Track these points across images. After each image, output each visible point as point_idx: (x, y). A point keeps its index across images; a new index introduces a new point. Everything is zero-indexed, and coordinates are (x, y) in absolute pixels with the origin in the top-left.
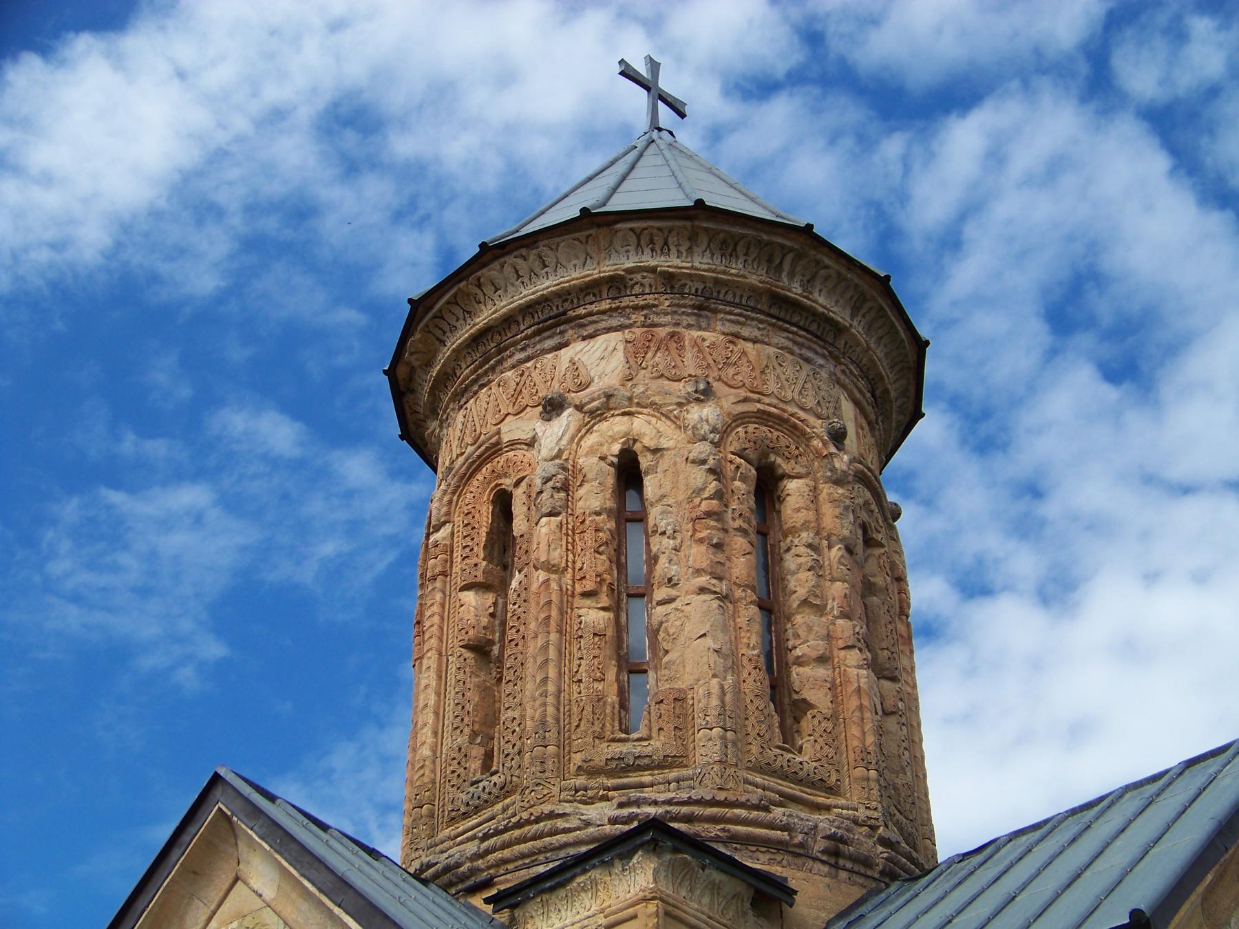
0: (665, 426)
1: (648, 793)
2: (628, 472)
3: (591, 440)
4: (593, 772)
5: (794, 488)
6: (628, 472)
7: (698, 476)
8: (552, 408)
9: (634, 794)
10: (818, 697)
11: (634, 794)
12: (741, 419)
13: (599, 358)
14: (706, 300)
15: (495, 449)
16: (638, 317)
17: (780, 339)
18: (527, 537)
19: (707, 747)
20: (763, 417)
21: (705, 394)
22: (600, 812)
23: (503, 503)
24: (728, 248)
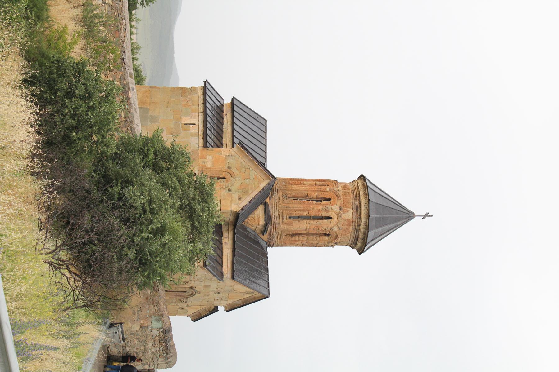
0: (334, 223)
1: (278, 220)
2: (329, 218)
3: (334, 213)
4: (282, 213)
5: (327, 237)
6: (329, 218)
7: (325, 228)
8: (340, 209)
9: (278, 218)
10: (293, 239)
11: (278, 218)
12: (336, 233)
13: (349, 214)
14: (357, 230)
15: (338, 199)
16: (354, 220)
17: (352, 238)
18: (321, 204)
19: (283, 227)
20: (337, 235)
21: (339, 229)
22: (276, 214)
23: (329, 200)
24: (364, 234)
